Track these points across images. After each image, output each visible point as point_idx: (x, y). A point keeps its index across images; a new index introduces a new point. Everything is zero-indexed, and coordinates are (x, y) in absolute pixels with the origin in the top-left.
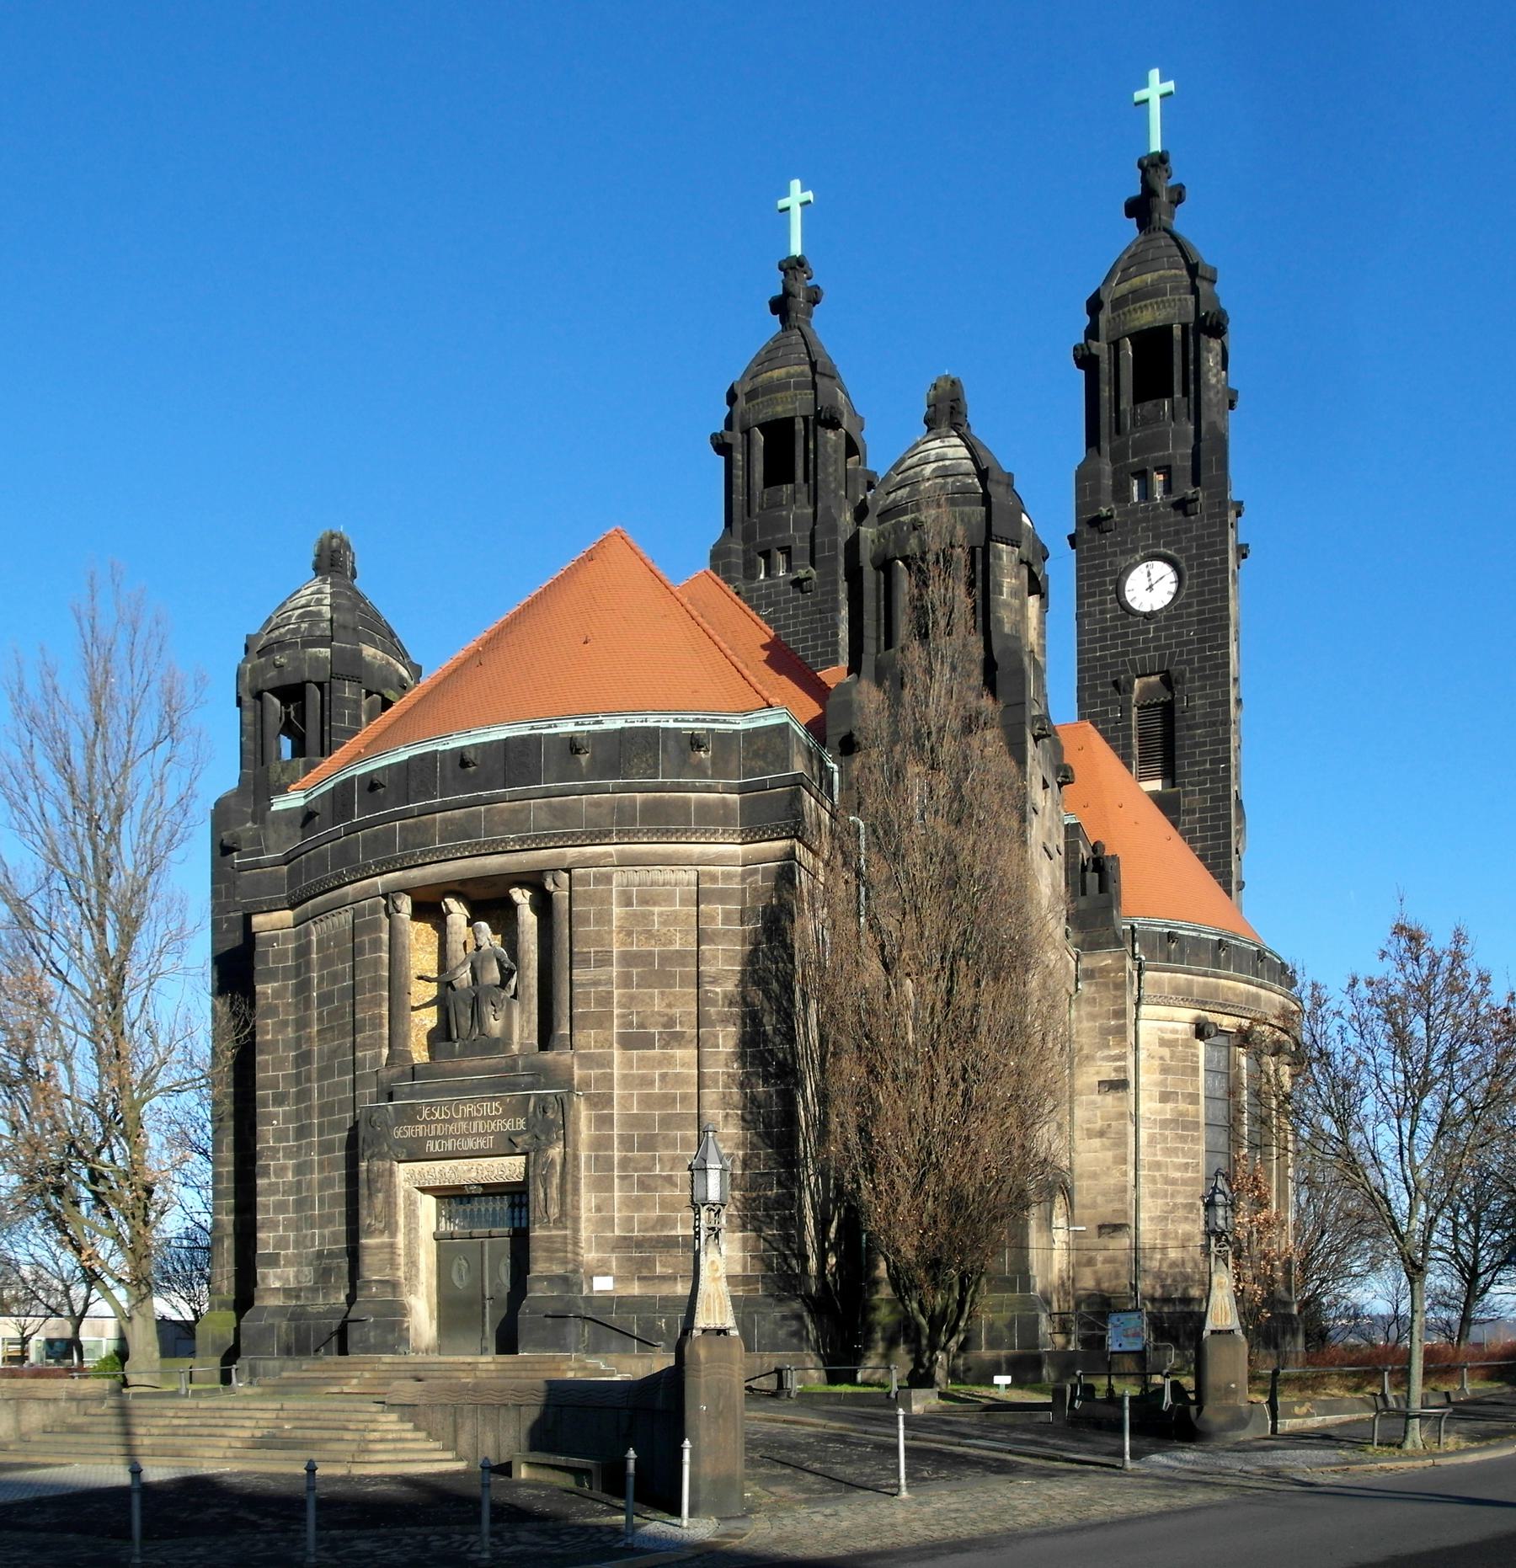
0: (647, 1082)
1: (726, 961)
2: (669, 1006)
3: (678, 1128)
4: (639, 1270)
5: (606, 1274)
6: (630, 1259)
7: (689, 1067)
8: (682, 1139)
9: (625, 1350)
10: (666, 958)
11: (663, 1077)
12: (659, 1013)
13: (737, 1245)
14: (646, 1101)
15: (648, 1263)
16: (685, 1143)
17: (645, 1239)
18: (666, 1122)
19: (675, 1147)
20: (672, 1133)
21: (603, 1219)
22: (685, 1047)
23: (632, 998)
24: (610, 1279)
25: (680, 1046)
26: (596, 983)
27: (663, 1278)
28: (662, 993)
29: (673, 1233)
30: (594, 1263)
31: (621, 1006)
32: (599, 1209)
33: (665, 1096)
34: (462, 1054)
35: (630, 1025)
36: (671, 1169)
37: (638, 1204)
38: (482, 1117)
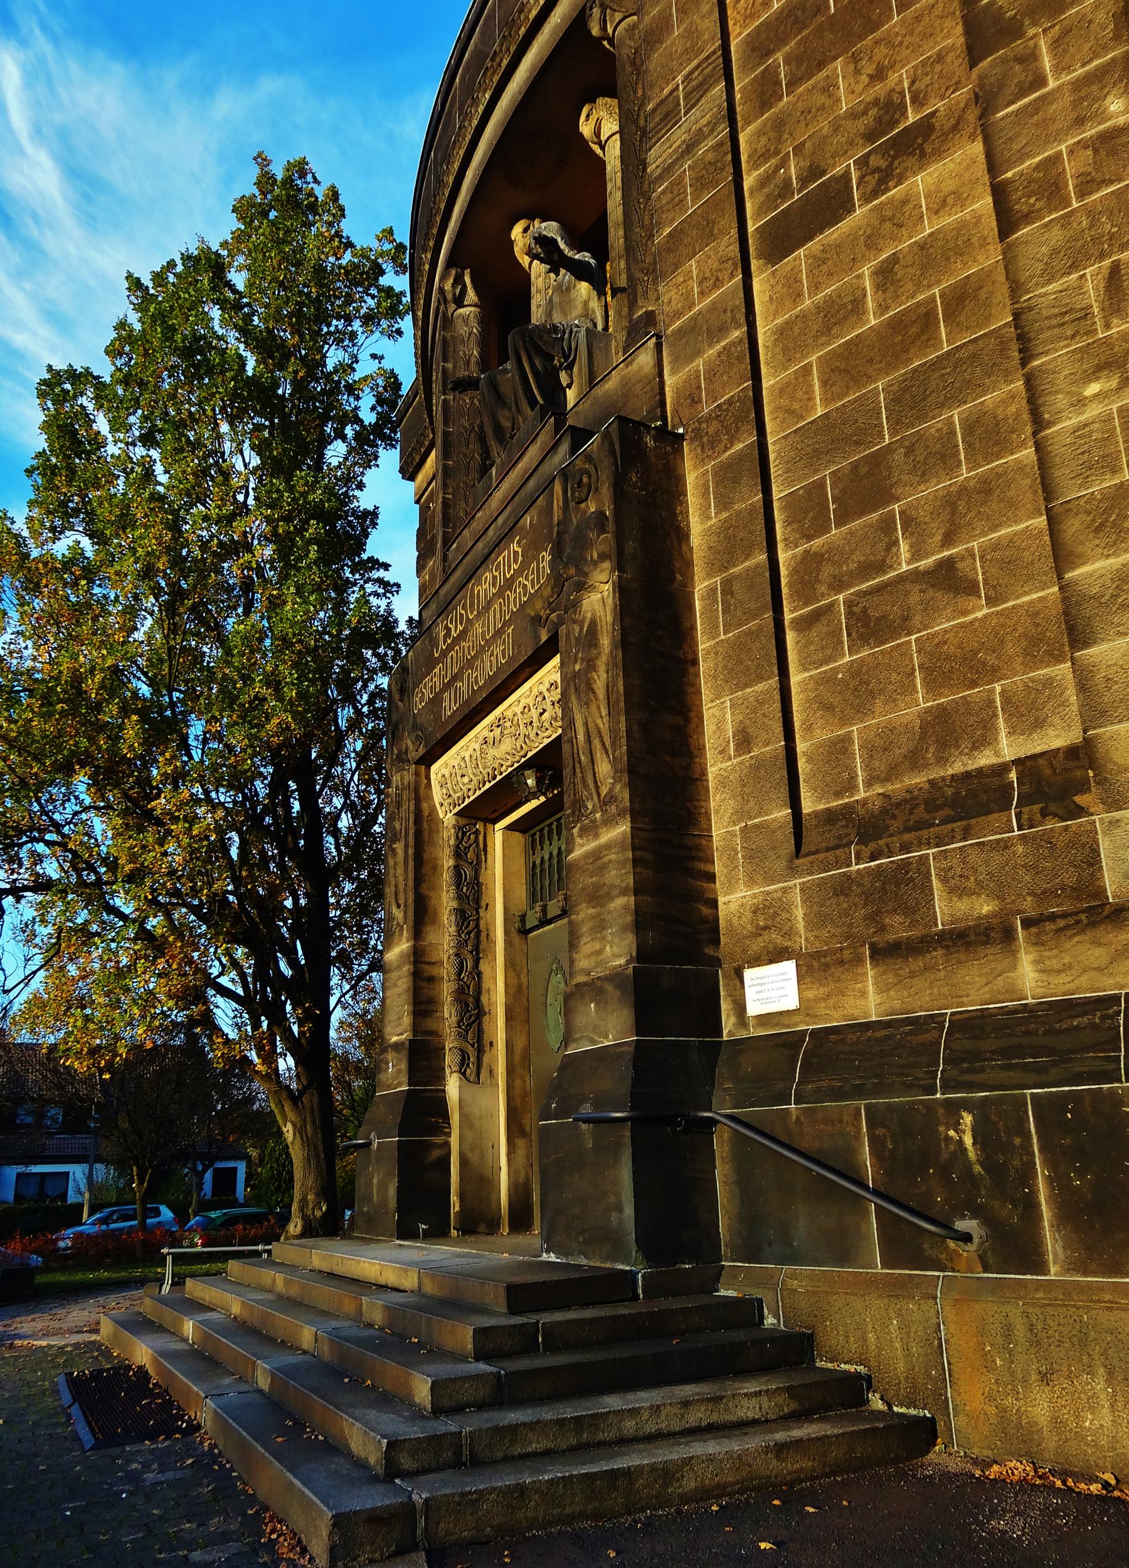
2: (879, 75)
4: (873, 918)
5: (776, 956)
6: (843, 887)
9: (842, 1250)
12: (853, 115)
15: (902, 888)
16: (988, 436)
17: (891, 807)
18: (910, 401)
19: (946, 459)
20: (932, 425)
21: (758, 766)
22: (939, 153)
24: (789, 967)
25: (924, 158)
27: (965, 939)
29: (985, 759)
30: (746, 924)
32: (744, 741)
33: (897, 325)
35: (785, 189)
36: (948, 540)
37: (855, 693)
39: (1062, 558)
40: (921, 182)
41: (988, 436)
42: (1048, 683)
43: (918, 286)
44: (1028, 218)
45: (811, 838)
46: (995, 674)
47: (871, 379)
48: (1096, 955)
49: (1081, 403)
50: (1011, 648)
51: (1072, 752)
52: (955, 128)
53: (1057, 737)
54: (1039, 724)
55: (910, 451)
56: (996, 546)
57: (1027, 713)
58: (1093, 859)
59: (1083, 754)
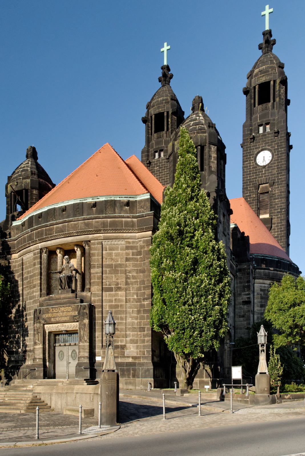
0: (111, 301)
1: (133, 266)
2: (117, 279)
3: (120, 314)
7: (123, 297)
8: (121, 317)
10: (116, 266)
11: (115, 299)
12: (114, 281)
13: (135, 348)
14: (111, 307)
16: (122, 319)
20: (118, 316)
23: (107, 277)
25: (120, 291)
26: (97, 273)
28: (115, 276)
29: (118, 344)
31: (105, 280)
33: (116, 305)
34: (61, 294)
35: (107, 285)
38: (66, 311)
39: (126, 331)
40: (120, 293)
41: (122, 319)
42: (123, 340)
43: (118, 303)
44: (128, 302)
45: (103, 347)
46: (119, 338)
47: (113, 309)
48: (124, 359)
49: (129, 320)
50: (121, 336)
51: (124, 345)
52: (123, 289)
53: (123, 344)
54: (122, 342)
55: (115, 317)
56: (121, 328)
57: (121, 341)
58: (124, 353)
59: (125, 346)
